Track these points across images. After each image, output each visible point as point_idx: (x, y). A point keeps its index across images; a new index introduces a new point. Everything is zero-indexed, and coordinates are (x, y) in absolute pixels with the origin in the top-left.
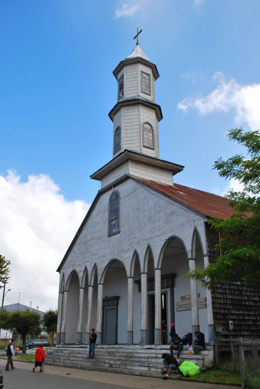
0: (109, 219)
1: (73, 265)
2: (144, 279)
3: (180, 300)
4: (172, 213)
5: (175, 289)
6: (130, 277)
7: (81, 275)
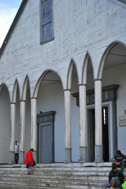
0: (41, 23)
1: (2, 78)
2: (82, 91)
3: (124, 114)
4: (115, 15)
5: (118, 102)
6: (67, 90)
7: (11, 89)
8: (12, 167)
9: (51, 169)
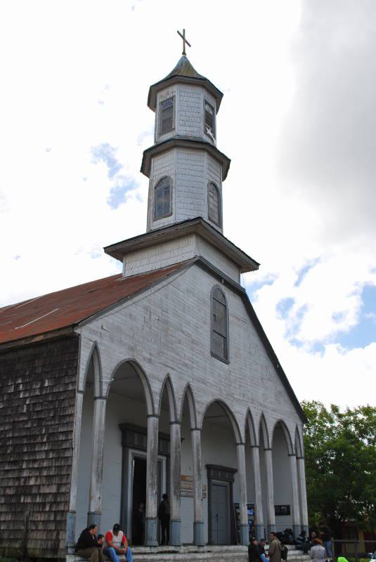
8: (158, 553)
9: (231, 555)
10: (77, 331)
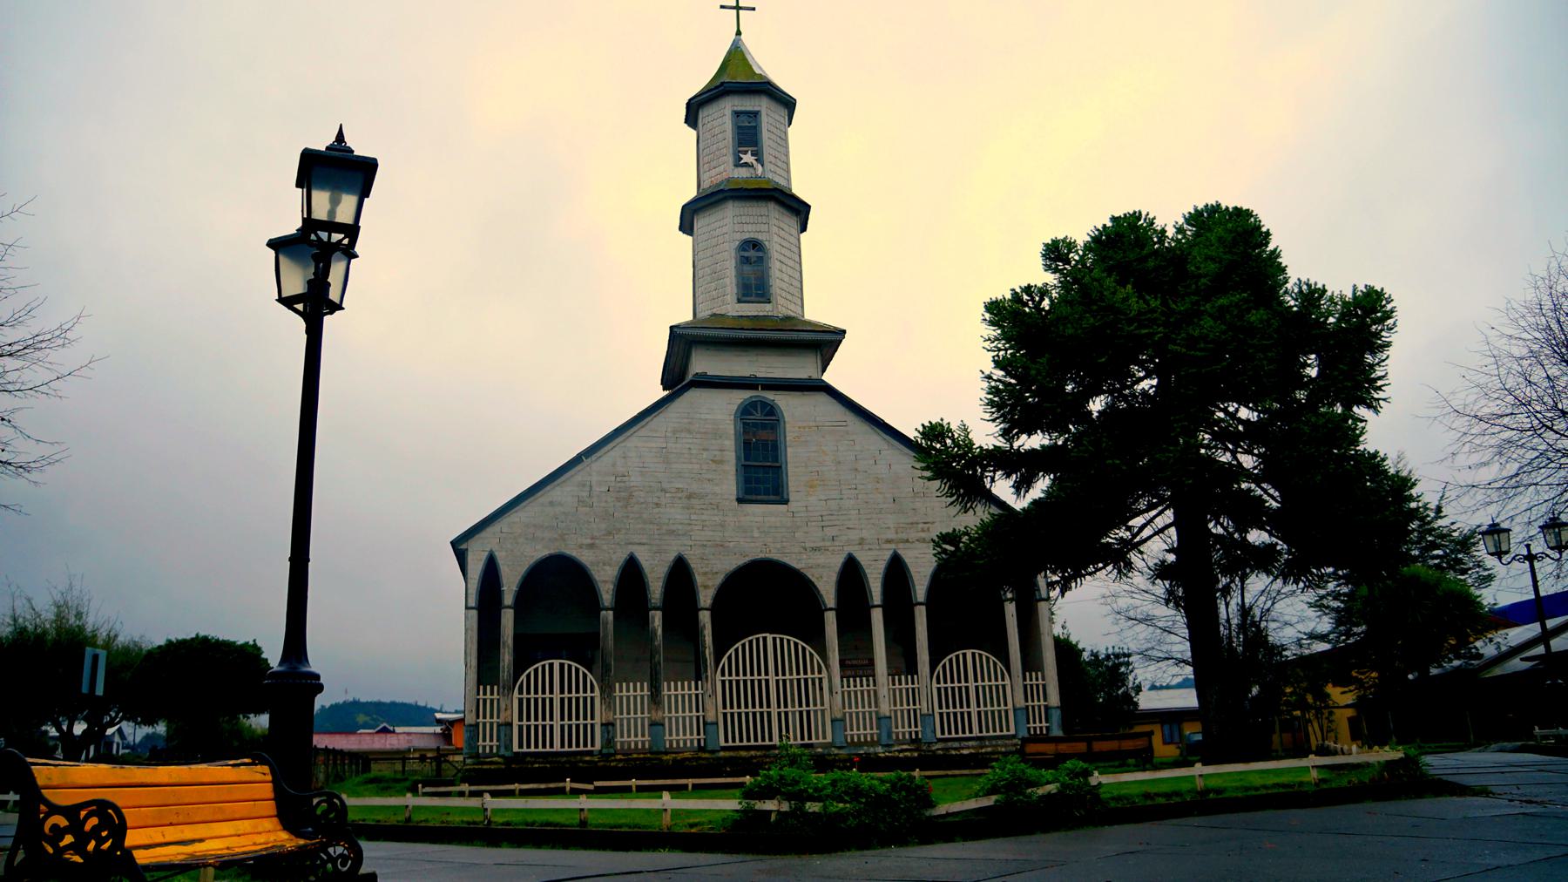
10: (463, 547)
